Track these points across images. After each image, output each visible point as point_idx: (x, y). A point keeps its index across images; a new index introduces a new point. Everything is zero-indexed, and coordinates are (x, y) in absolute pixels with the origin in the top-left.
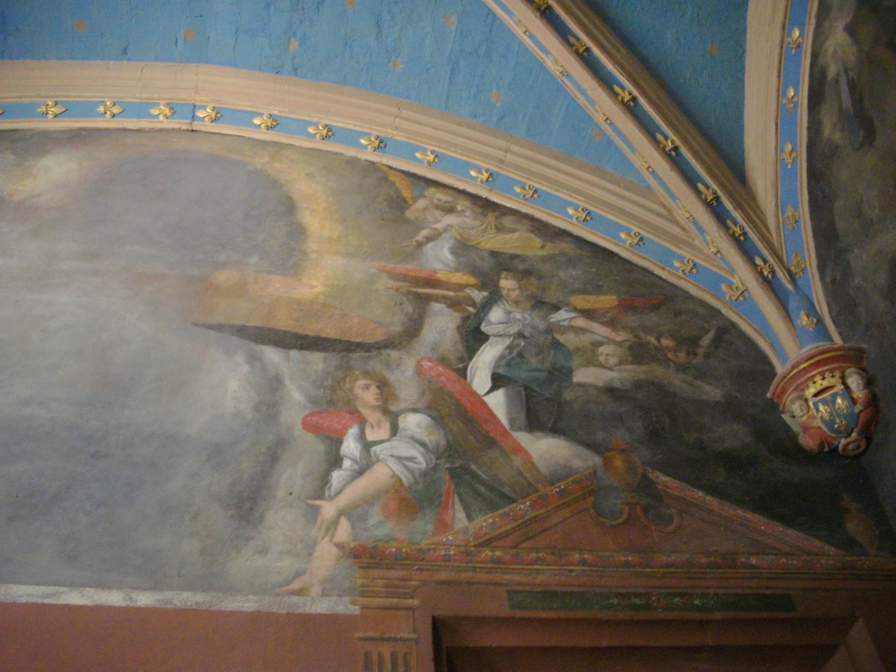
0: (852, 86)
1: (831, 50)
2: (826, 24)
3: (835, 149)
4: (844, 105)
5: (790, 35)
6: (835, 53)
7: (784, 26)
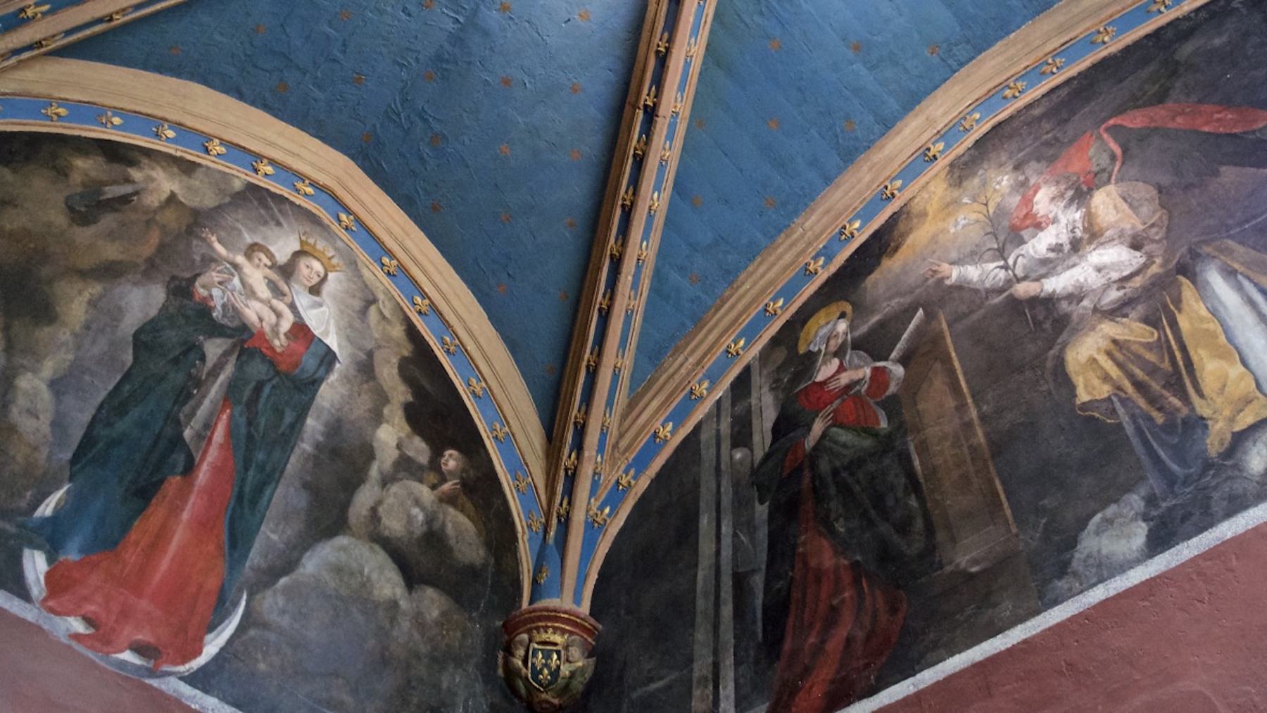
0: (125, 200)
1: (153, 174)
2: (176, 170)
3: (63, 173)
4: (107, 188)
5: (170, 128)
6: (152, 180)
7: (180, 124)
